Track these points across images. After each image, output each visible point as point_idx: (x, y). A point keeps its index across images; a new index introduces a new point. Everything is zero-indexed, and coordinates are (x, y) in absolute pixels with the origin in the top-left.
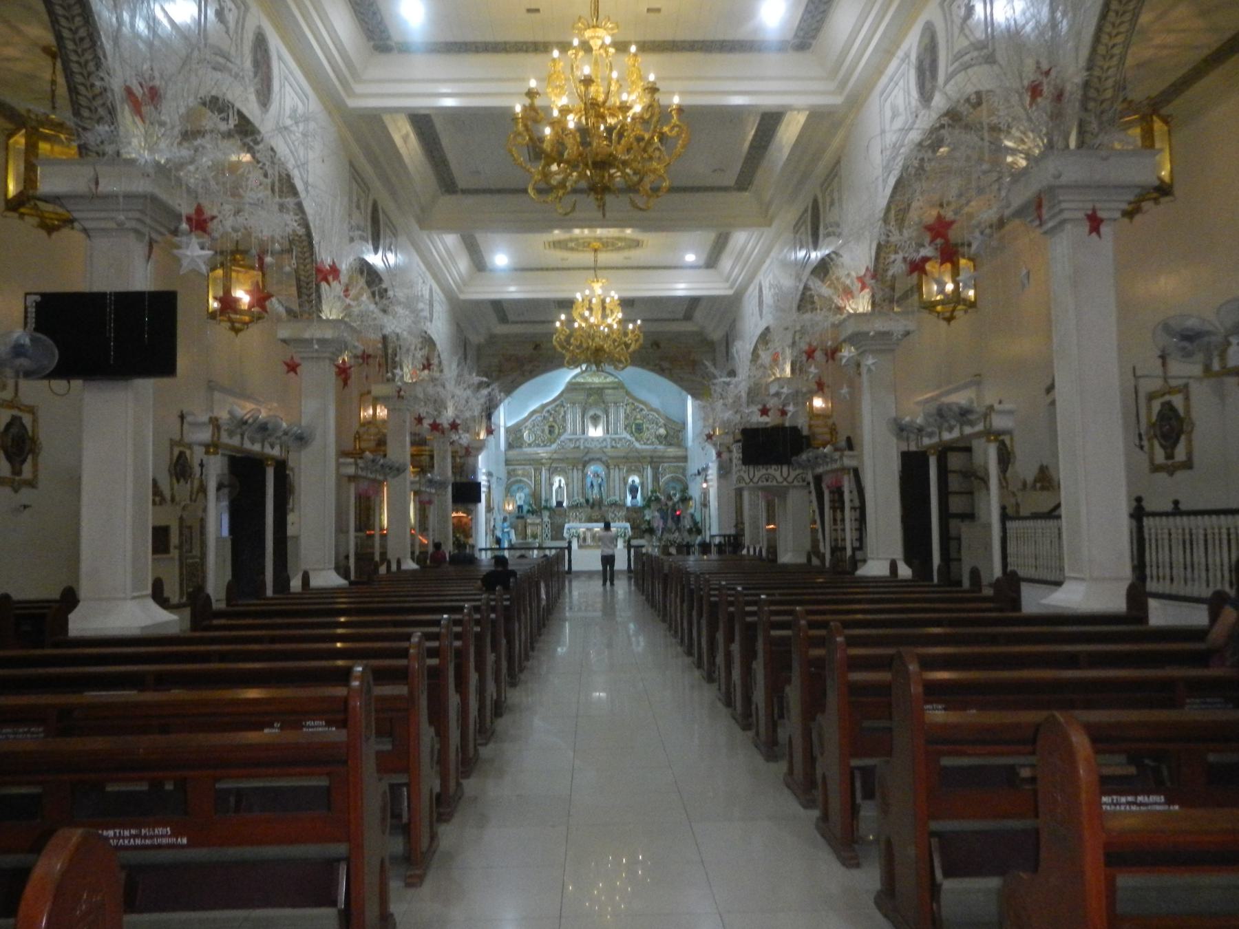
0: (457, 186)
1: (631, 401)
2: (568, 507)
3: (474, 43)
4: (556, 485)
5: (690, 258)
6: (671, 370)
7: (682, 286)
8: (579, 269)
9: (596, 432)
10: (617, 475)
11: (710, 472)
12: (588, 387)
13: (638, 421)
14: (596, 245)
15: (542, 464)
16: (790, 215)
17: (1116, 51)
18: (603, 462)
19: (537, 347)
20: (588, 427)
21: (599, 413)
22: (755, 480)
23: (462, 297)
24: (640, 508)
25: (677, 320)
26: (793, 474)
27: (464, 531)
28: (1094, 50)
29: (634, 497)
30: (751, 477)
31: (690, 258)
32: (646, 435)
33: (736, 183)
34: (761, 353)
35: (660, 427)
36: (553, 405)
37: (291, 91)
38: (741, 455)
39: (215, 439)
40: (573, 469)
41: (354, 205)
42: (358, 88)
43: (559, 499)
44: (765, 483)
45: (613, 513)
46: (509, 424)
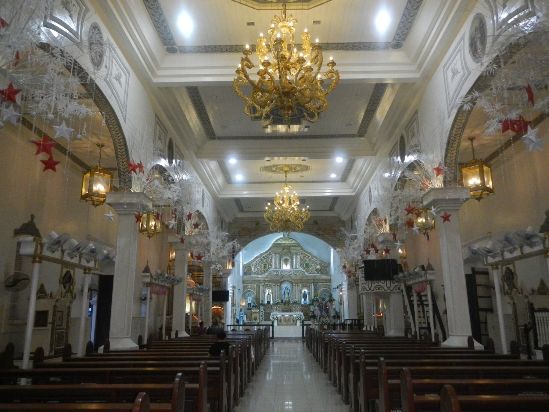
0: (215, 135)
1: (303, 252)
3: (220, 46)
4: (267, 293)
6: (323, 235)
8: (278, 182)
9: (286, 267)
10: (297, 289)
11: (343, 286)
12: (283, 245)
13: (307, 262)
14: (286, 169)
15: (260, 283)
16: (387, 148)
18: (290, 282)
19: (257, 224)
21: (288, 258)
22: (372, 289)
23: (220, 196)
25: (327, 210)
26: (393, 285)
27: (218, 316)
29: (305, 300)
30: (370, 287)
32: (311, 269)
33: (358, 133)
34: (373, 220)
35: (318, 265)
36: (266, 254)
37: (116, 64)
39: (39, 251)
40: (275, 286)
41: (157, 137)
42: (159, 73)
43: (268, 300)
44: (378, 291)
46: (245, 263)
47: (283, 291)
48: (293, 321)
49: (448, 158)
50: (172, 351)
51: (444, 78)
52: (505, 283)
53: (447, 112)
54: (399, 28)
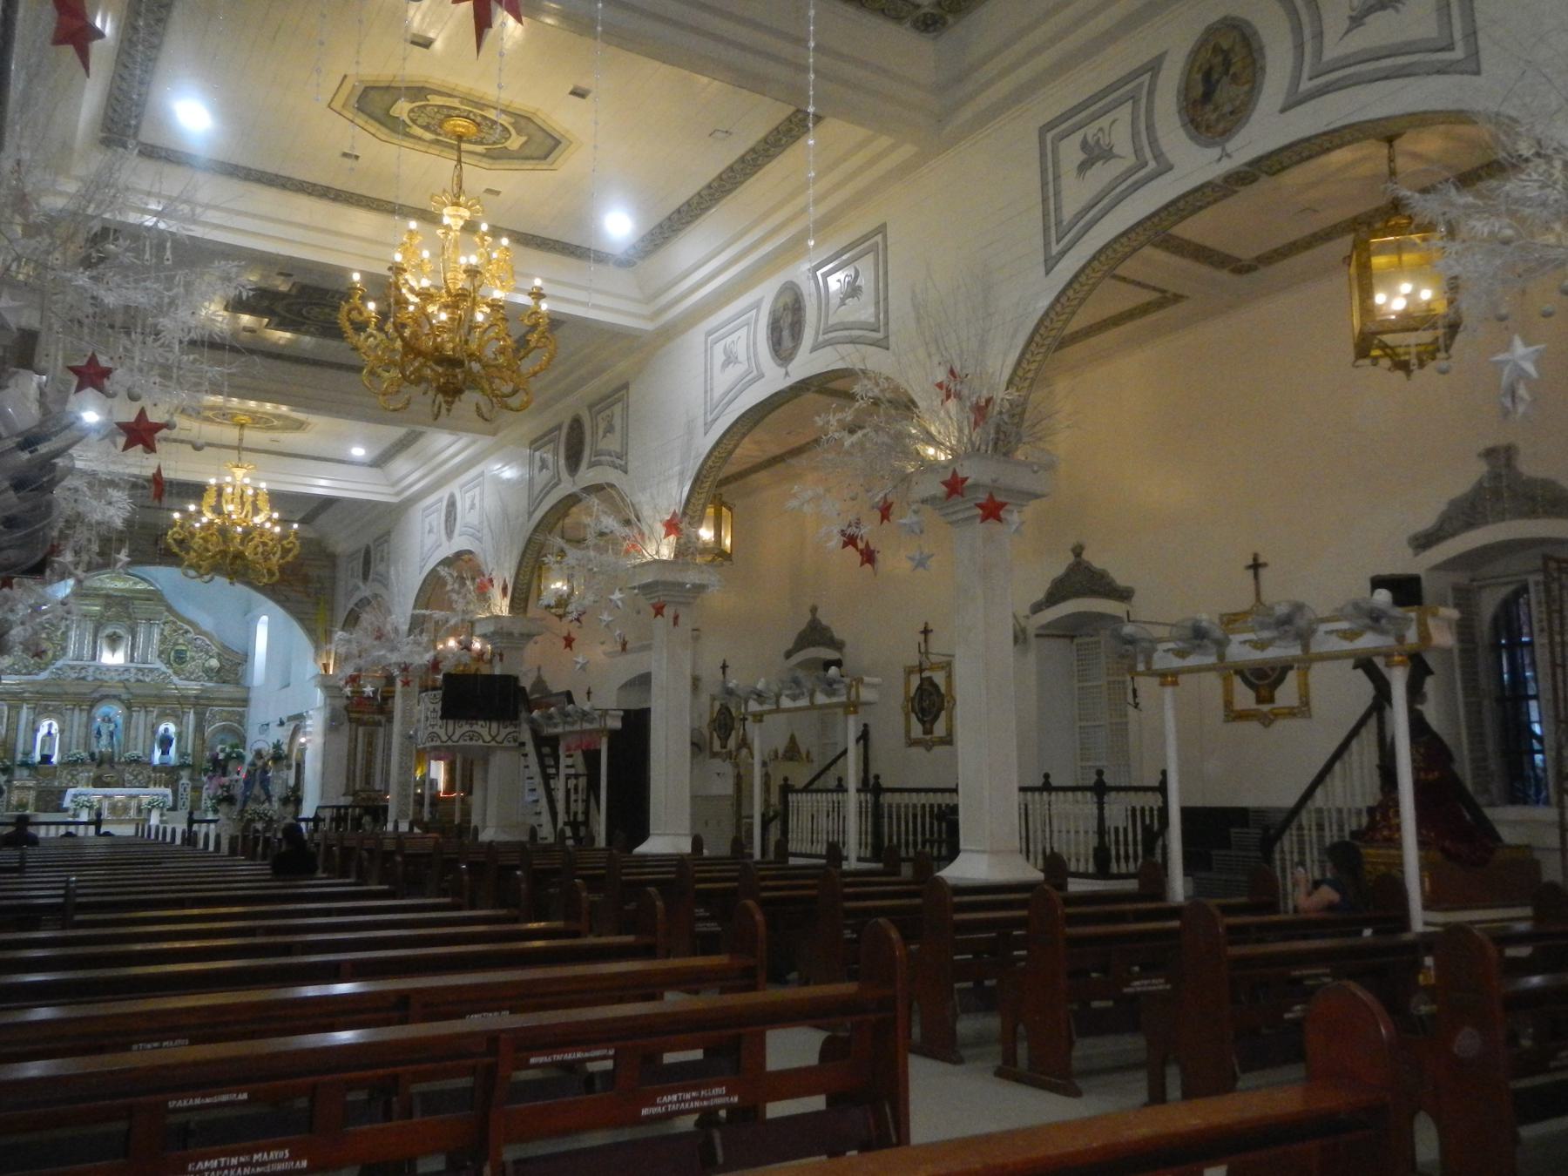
1: (171, 618)
2: (60, 763)
4: (43, 731)
5: (358, 452)
7: (323, 482)
9: (113, 658)
10: (142, 723)
14: (244, 419)
17: (1030, 375)
18: (120, 700)
20: (101, 652)
21: (120, 631)
22: (455, 738)
24: (173, 767)
26: (504, 732)
28: (1015, 372)
29: (165, 752)
31: (358, 452)
32: (190, 666)
35: (211, 657)
38: (438, 707)
40: (73, 710)
44: (468, 743)
45: (131, 774)
47: (95, 727)
48: (139, 810)
49: (691, 506)
50: (12, 883)
51: (706, 356)
52: (715, 735)
53: (703, 423)
54: (642, 240)
